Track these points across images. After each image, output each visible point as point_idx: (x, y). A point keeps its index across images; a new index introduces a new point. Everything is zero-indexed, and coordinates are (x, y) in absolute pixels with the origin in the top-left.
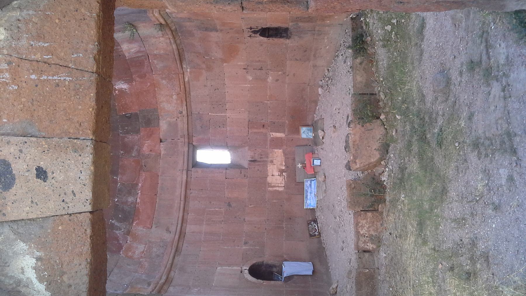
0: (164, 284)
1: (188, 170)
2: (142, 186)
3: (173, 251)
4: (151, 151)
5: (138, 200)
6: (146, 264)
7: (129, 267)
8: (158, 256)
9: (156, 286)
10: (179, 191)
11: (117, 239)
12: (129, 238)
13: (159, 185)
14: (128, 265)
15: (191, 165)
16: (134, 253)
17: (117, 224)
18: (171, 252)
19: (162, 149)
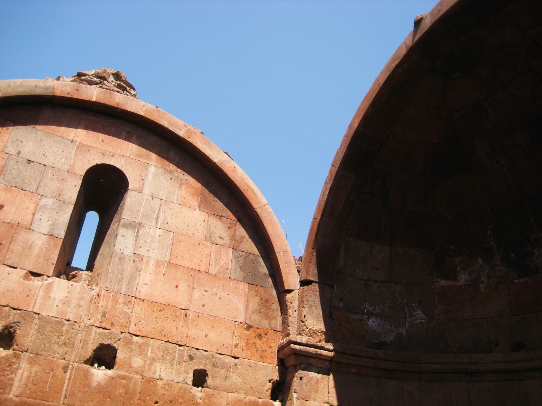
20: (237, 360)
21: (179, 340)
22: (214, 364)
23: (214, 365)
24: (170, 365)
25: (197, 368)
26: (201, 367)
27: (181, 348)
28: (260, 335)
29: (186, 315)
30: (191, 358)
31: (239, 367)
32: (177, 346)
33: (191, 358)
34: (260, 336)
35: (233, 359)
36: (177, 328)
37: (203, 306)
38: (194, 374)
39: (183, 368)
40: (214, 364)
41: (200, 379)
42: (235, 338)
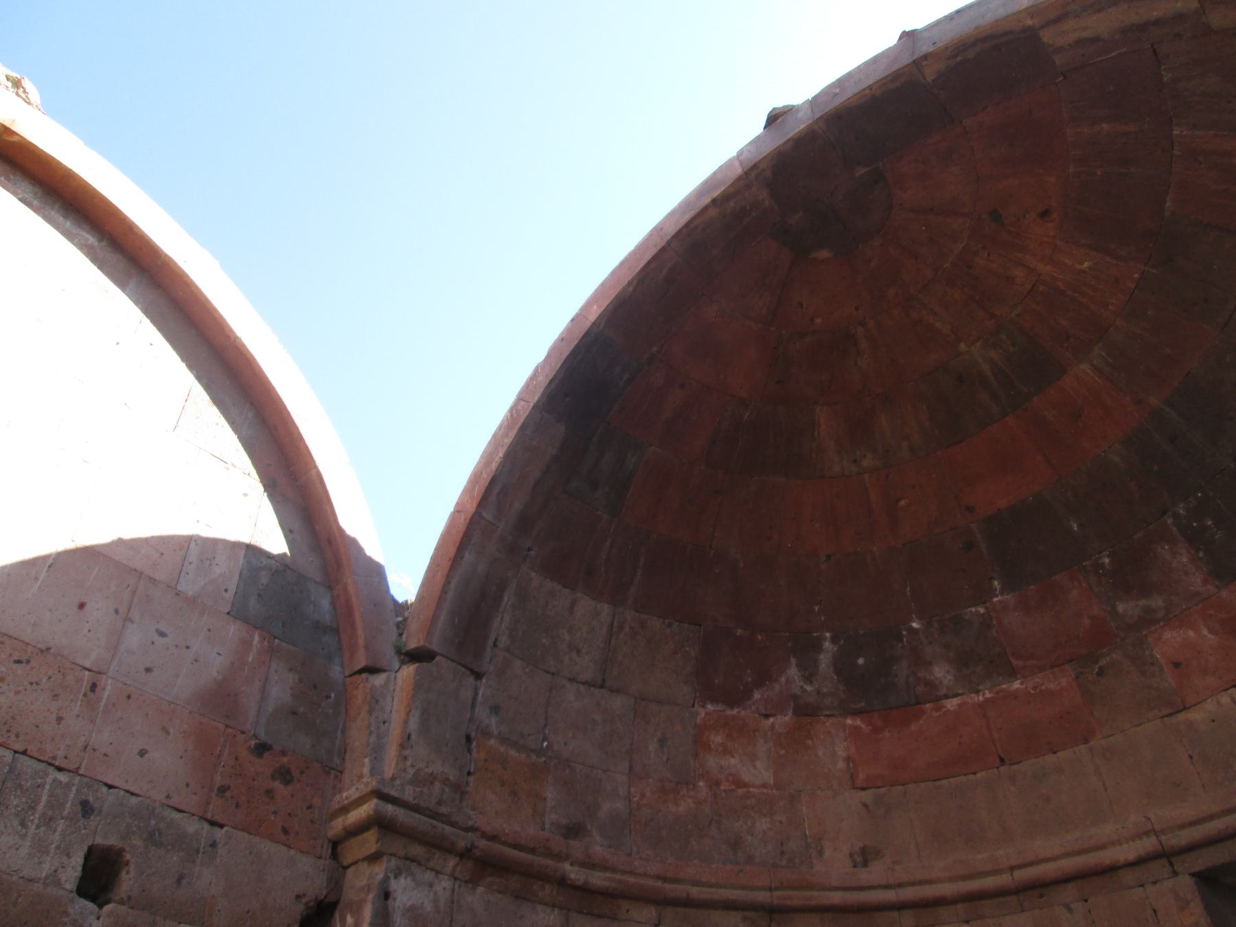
0: (562, 882)
1: (1166, 855)
2: (1013, 695)
3: (762, 897)
4: (1177, 665)
5: (952, 704)
6: (685, 805)
7: (653, 747)
8: (736, 844)
9: (532, 851)
10: (1051, 852)
11: (764, 678)
12: (783, 720)
13: (1050, 759)
14: (662, 741)
15: (1203, 861)
16: (726, 751)
17: (825, 660)
18: (753, 888)
19: (1210, 705)
20: (219, 834)
21: (61, 754)
22: (151, 835)
23: (153, 838)
24: (16, 822)
25: (99, 840)
26: (113, 841)
27: (63, 777)
28: (288, 772)
29: (94, 687)
30: (86, 809)
31: (221, 851)
32: (51, 769)
33: (86, 809)
34: (284, 775)
35: (206, 826)
36: (60, 719)
37: (148, 670)
38: (87, 858)
39: (57, 837)
40: (151, 835)
41: (99, 877)
42: (221, 769)
